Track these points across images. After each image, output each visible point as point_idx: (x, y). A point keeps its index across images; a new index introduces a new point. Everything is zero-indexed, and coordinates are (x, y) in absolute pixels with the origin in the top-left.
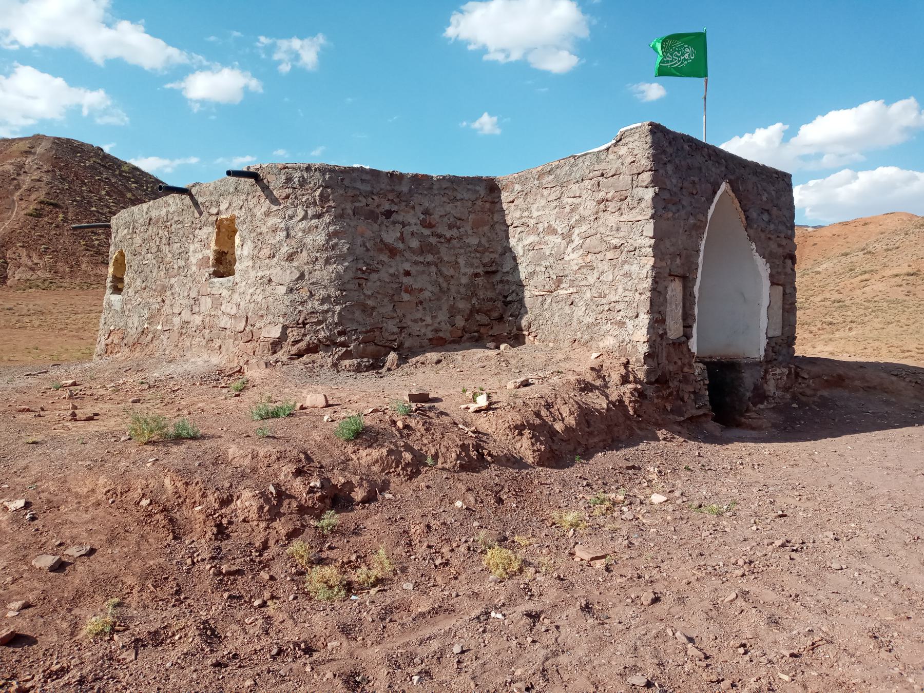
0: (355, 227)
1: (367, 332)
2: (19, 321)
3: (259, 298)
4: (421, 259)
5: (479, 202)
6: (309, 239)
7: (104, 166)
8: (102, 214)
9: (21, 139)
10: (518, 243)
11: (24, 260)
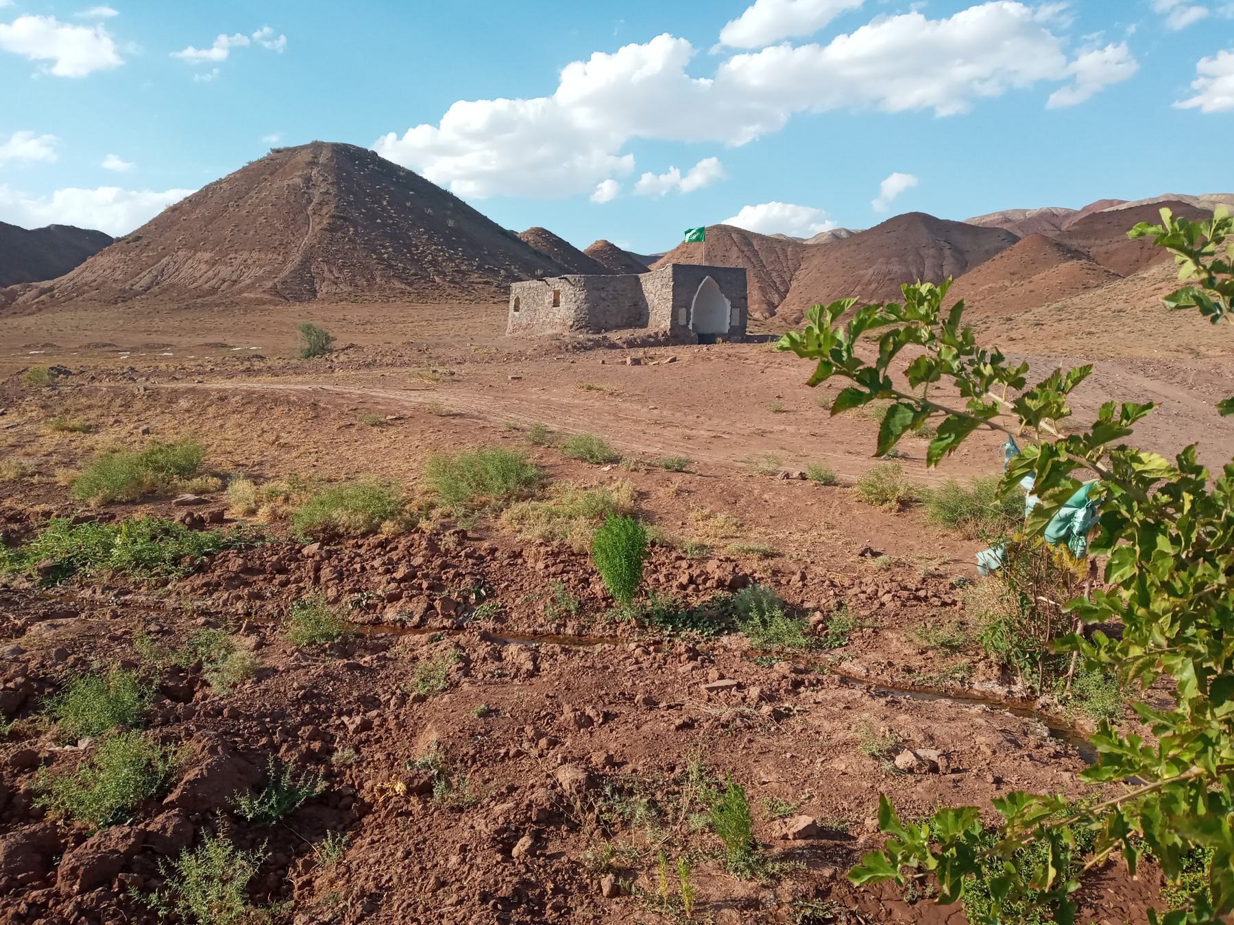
11: (327, 274)
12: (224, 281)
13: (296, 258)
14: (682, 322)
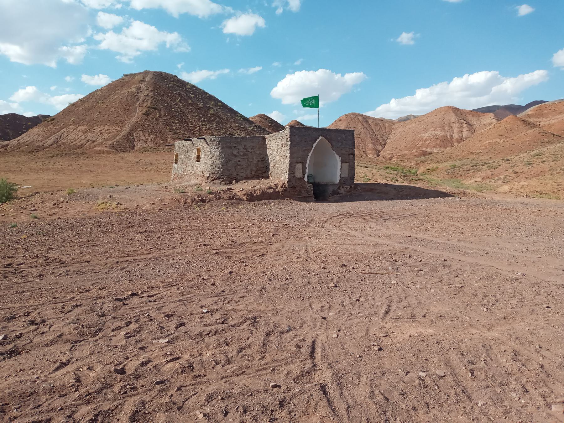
2: (142, 168)
6: (215, 154)
7: (178, 86)
11: (142, 137)
12: (89, 141)
13: (127, 129)
14: (299, 174)
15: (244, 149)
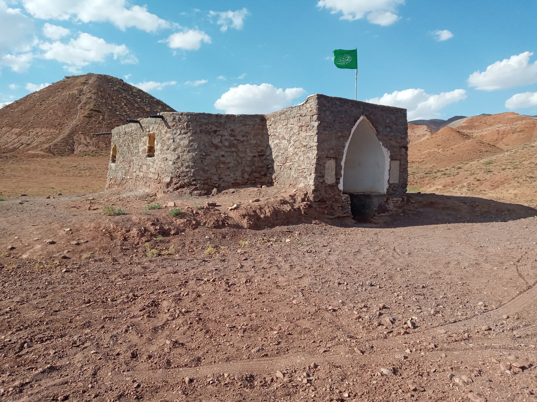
0: (201, 138)
1: (205, 180)
2: (79, 173)
3: (162, 166)
4: (229, 150)
5: (257, 126)
7: (123, 90)
8: (122, 116)
9: (81, 76)
10: (272, 143)
11: (83, 140)
12: (22, 144)
13: (67, 131)
14: (330, 179)
15: (231, 135)
